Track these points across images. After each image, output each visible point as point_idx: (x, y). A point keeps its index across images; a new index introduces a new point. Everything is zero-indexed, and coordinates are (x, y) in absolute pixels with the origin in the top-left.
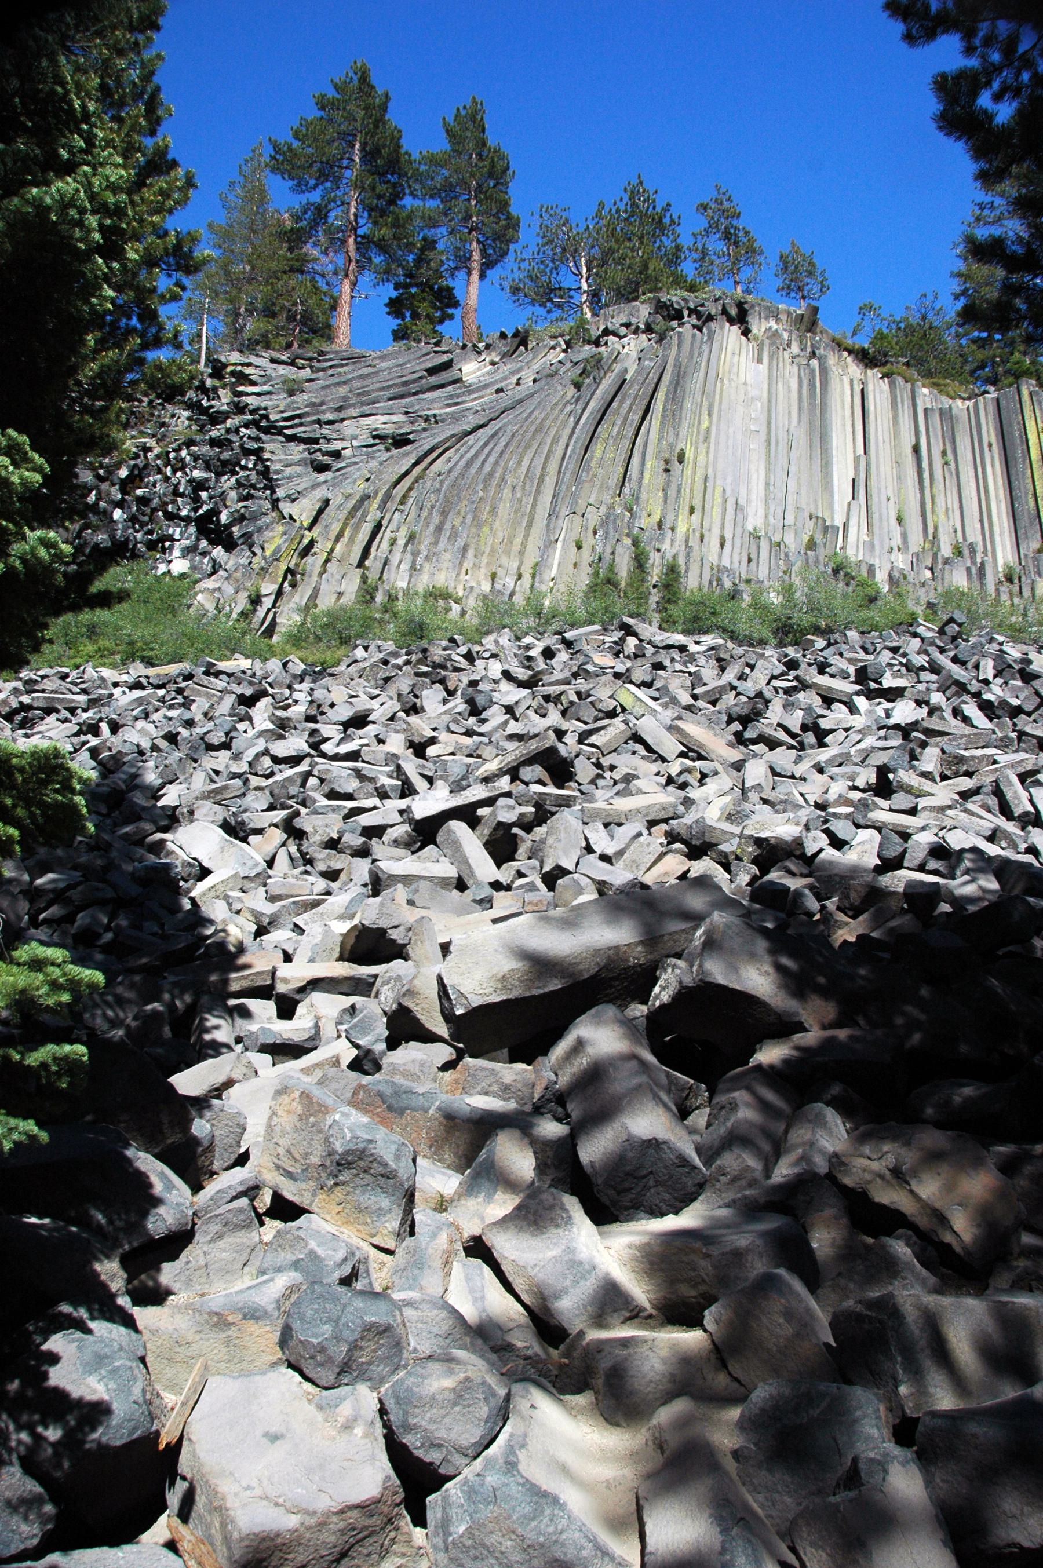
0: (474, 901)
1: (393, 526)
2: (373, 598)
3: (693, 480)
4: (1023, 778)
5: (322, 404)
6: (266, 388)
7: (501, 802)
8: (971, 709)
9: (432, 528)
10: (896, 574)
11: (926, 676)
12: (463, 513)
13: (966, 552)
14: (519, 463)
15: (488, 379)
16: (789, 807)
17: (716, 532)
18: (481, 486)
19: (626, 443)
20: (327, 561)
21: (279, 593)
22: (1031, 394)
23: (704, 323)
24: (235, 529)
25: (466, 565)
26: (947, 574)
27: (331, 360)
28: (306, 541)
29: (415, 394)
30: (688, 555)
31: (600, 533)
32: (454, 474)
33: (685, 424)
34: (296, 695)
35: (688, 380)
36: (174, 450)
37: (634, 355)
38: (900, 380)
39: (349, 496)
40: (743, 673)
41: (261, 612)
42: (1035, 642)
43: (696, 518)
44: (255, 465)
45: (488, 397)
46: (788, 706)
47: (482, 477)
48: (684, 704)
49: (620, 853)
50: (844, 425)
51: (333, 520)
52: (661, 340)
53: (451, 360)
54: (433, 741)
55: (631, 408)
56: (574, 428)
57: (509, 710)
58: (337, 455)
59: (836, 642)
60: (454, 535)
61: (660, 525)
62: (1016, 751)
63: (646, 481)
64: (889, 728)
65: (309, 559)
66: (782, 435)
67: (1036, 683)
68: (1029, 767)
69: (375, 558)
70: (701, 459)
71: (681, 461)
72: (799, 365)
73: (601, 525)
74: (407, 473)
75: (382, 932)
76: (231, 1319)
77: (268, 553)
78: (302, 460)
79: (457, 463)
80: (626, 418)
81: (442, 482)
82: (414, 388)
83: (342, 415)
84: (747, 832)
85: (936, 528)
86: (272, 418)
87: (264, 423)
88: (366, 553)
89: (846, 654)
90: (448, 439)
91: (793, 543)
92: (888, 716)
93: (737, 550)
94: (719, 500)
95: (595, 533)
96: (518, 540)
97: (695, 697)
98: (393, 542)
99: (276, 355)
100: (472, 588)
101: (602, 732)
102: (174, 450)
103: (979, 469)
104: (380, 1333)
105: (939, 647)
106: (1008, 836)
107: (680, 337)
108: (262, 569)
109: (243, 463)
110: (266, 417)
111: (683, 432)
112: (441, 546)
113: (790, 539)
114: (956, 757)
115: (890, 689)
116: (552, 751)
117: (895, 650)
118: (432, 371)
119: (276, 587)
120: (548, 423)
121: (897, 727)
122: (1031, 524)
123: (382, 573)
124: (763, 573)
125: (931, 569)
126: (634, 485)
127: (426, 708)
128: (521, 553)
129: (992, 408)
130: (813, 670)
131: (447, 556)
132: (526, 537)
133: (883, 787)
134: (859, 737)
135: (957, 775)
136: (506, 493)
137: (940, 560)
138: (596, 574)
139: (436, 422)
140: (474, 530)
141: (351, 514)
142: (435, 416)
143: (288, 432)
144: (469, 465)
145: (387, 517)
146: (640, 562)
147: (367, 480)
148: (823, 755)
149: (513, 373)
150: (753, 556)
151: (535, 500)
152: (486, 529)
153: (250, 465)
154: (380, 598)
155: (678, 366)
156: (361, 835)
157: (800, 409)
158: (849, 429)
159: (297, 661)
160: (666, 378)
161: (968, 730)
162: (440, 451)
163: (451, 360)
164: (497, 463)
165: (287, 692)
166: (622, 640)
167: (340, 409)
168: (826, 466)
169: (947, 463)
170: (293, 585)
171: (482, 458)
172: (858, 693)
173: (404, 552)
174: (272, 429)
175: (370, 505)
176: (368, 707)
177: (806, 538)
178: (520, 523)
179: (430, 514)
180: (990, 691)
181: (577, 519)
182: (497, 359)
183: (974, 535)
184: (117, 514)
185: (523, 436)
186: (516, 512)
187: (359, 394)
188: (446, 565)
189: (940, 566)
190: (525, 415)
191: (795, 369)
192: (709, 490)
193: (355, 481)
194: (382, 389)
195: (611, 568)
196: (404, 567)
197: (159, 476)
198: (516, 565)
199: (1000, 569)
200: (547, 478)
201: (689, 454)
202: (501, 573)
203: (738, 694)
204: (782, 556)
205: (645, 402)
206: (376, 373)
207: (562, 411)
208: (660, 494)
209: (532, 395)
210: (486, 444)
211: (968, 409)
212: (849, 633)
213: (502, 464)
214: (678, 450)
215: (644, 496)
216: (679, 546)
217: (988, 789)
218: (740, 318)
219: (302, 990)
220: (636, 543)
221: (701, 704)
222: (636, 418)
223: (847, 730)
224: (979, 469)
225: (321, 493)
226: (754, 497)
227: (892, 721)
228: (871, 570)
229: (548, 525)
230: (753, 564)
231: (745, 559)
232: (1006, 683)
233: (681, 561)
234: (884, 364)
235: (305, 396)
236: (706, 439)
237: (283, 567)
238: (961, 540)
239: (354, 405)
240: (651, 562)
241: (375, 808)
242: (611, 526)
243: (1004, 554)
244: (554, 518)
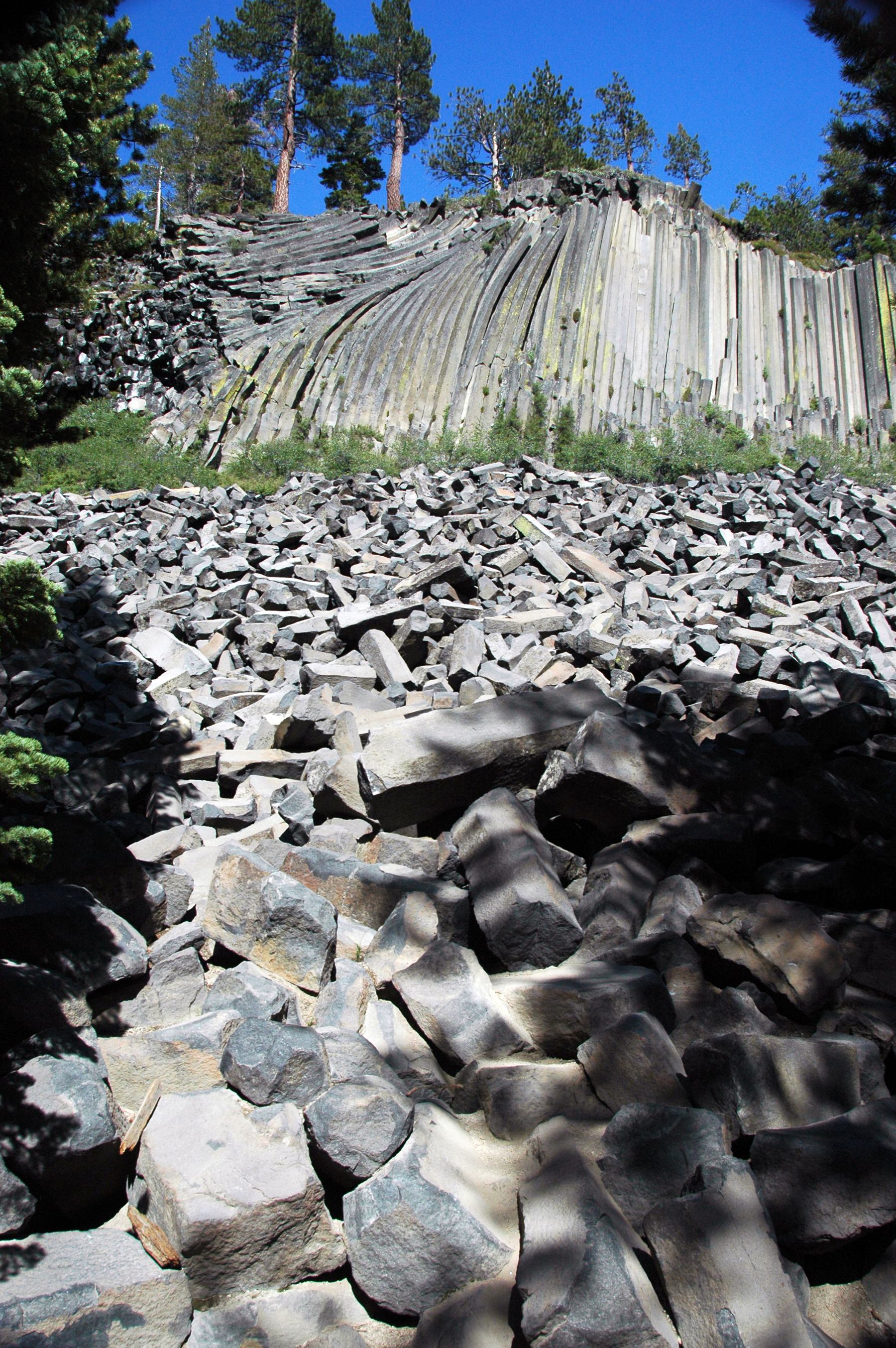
0: (391, 699)
1: (324, 372)
2: (306, 435)
3: (587, 338)
4: (863, 603)
5: (263, 263)
6: (214, 248)
7: (415, 614)
8: (821, 543)
9: (358, 374)
10: (760, 423)
11: (783, 513)
12: (385, 362)
13: (822, 406)
14: (435, 319)
15: (409, 244)
16: (662, 623)
17: (605, 383)
18: (401, 338)
19: (529, 303)
20: (266, 402)
21: (224, 430)
22: (884, 268)
23: (600, 197)
24: (186, 373)
25: (388, 407)
26: (804, 426)
27: (271, 224)
28: (248, 384)
29: (345, 255)
30: (581, 402)
31: (505, 381)
32: (379, 327)
33: (581, 287)
34: (238, 519)
35: (585, 247)
36: (132, 302)
37: (538, 224)
38: (770, 252)
39: (285, 346)
40: (626, 507)
41: (208, 446)
42: (879, 485)
43: (588, 370)
44: (204, 316)
45: (409, 259)
46: (663, 536)
47: (402, 331)
48: (574, 532)
49: (516, 660)
50: (720, 292)
51: (272, 367)
52: (561, 213)
53: (377, 226)
54: (356, 560)
55: (533, 272)
56: (484, 288)
57: (423, 534)
58: (275, 308)
59: (707, 482)
60: (377, 381)
61: (557, 376)
62: (858, 580)
63: (545, 336)
64: (750, 557)
65: (251, 400)
66: (665, 299)
67: (877, 521)
68: (869, 594)
69: (308, 400)
70: (594, 318)
72: (682, 237)
73: (506, 375)
74: (337, 326)
75: (311, 724)
76: (180, 1048)
77: (215, 394)
78: (244, 312)
79: (381, 317)
80: (529, 281)
81: (367, 334)
82: (343, 249)
83: (280, 273)
84: (625, 644)
85: (797, 384)
86: (219, 274)
87: (212, 279)
88: (300, 395)
89: (715, 493)
90: (373, 296)
91: (672, 394)
92: (750, 547)
93: (623, 400)
94: (609, 355)
95: (500, 381)
96: (433, 387)
97: (584, 527)
98: (324, 387)
99: (222, 218)
100: (392, 428)
101: (503, 555)
102: (132, 302)
103: (836, 334)
104: (306, 1060)
105: (795, 488)
106: (848, 653)
108: (210, 408)
109: (193, 314)
110: (213, 274)
111: (579, 294)
112: (366, 390)
113: (669, 391)
114: (806, 584)
115: (752, 523)
116: (459, 570)
117: (757, 490)
118: (360, 236)
119: (222, 424)
120: (460, 284)
121: (757, 556)
122: (880, 382)
123: (314, 413)
124: (645, 420)
125: (791, 420)
126: (535, 340)
127: (351, 531)
128: (436, 398)
129: (849, 279)
130: (687, 505)
131: (371, 399)
132: (440, 384)
133: (743, 608)
134: (724, 564)
135: (807, 599)
136: (424, 345)
137: (799, 412)
138: (500, 417)
139: (363, 281)
140: (394, 377)
141: (288, 361)
142: (362, 275)
143: (232, 287)
144: (391, 319)
145: (319, 364)
146: (539, 408)
147: (302, 331)
148: (693, 579)
149: (432, 239)
150: (637, 405)
151: (448, 352)
152: (405, 376)
153: (200, 317)
154: (312, 435)
155: (576, 235)
156: (294, 641)
157: (682, 276)
158: (724, 295)
159: (240, 489)
161: (818, 561)
162: (366, 306)
163: (377, 226)
164: (416, 318)
165: (230, 516)
166: (522, 475)
167: (278, 268)
168: (703, 327)
169: (808, 328)
170: (237, 423)
171: (402, 314)
172: (724, 526)
173: (333, 395)
174: (220, 285)
175: (304, 353)
176: (300, 530)
177: (684, 390)
178: (435, 372)
179: (357, 362)
180: (838, 527)
181: (485, 369)
182: (417, 226)
183: (829, 391)
184: (83, 358)
185: (439, 294)
186: (432, 361)
187: (295, 255)
188: (370, 407)
189: (799, 417)
190: (441, 276)
191: (679, 240)
192: (600, 346)
193: (291, 332)
194: (316, 251)
195: (514, 412)
196: (334, 408)
197: (119, 325)
198: (431, 408)
199: (851, 422)
200: (459, 333)
201: (584, 314)
202: (417, 415)
203: (621, 525)
204: (663, 406)
205: (546, 267)
206: (311, 236)
207: (473, 273)
208: (558, 348)
209: (447, 259)
210: (406, 301)
211: (829, 280)
212: (718, 474)
213: (420, 319)
214: (574, 310)
215: (543, 350)
216: (573, 394)
217: (833, 612)
218: (632, 194)
219: (241, 773)
220: (535, 391)
221: (588, 532)
222: (538, 281)
223: (713, 558)
224: (836, 334)
225: (262, 342)
226: (639, 352)
227: (753, 551)
228: (739, 419)
229: (459, 374)
230: (637, 412)
232: (852, 521)
233: (575, 408)
234: (756, 238)
235: (248, 256)
236: (599, 301)
237: (228, 407)
238: (818, 395)
239: (290, 265)
240: (548, 408)
241: (306, 618)
242: (514, 376)
243: (855, 409)
244: (464, 367)
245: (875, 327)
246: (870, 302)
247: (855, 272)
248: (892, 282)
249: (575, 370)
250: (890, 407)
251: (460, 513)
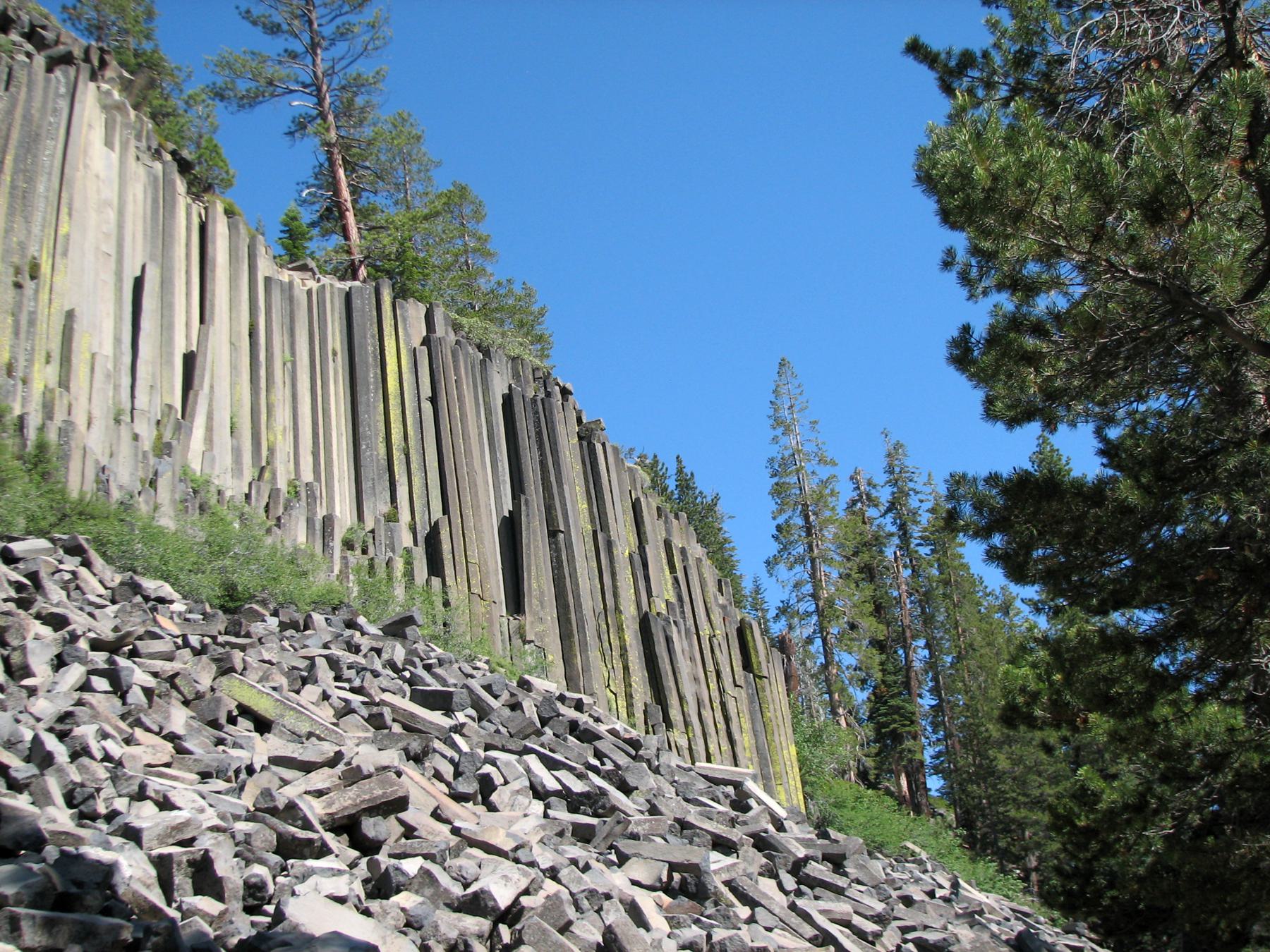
13: (303, 495)
26: (293, 523)
33: (38, 217)
67: (598, 744)
70: (57, 279)
71: (33, 277)
94: (88, 356)
107: (30, 74)
111: (36, 230)
122: (380, 478)
129: (339, 304)
155: (27, 117)
157: (145, 231)
160: (15, 135)
201: (45, 268)
208: (10, 320)
214: (30, 257)
231: (107, 452)
233: (52, 436)
236: (65, 254)
238: (293, 477)
245: (376, 390)
246: (370, 349)
247: (348, 296)
248: (405, 329)
249: (37, 367)
250: (397, 521)
251: (152, 656)
